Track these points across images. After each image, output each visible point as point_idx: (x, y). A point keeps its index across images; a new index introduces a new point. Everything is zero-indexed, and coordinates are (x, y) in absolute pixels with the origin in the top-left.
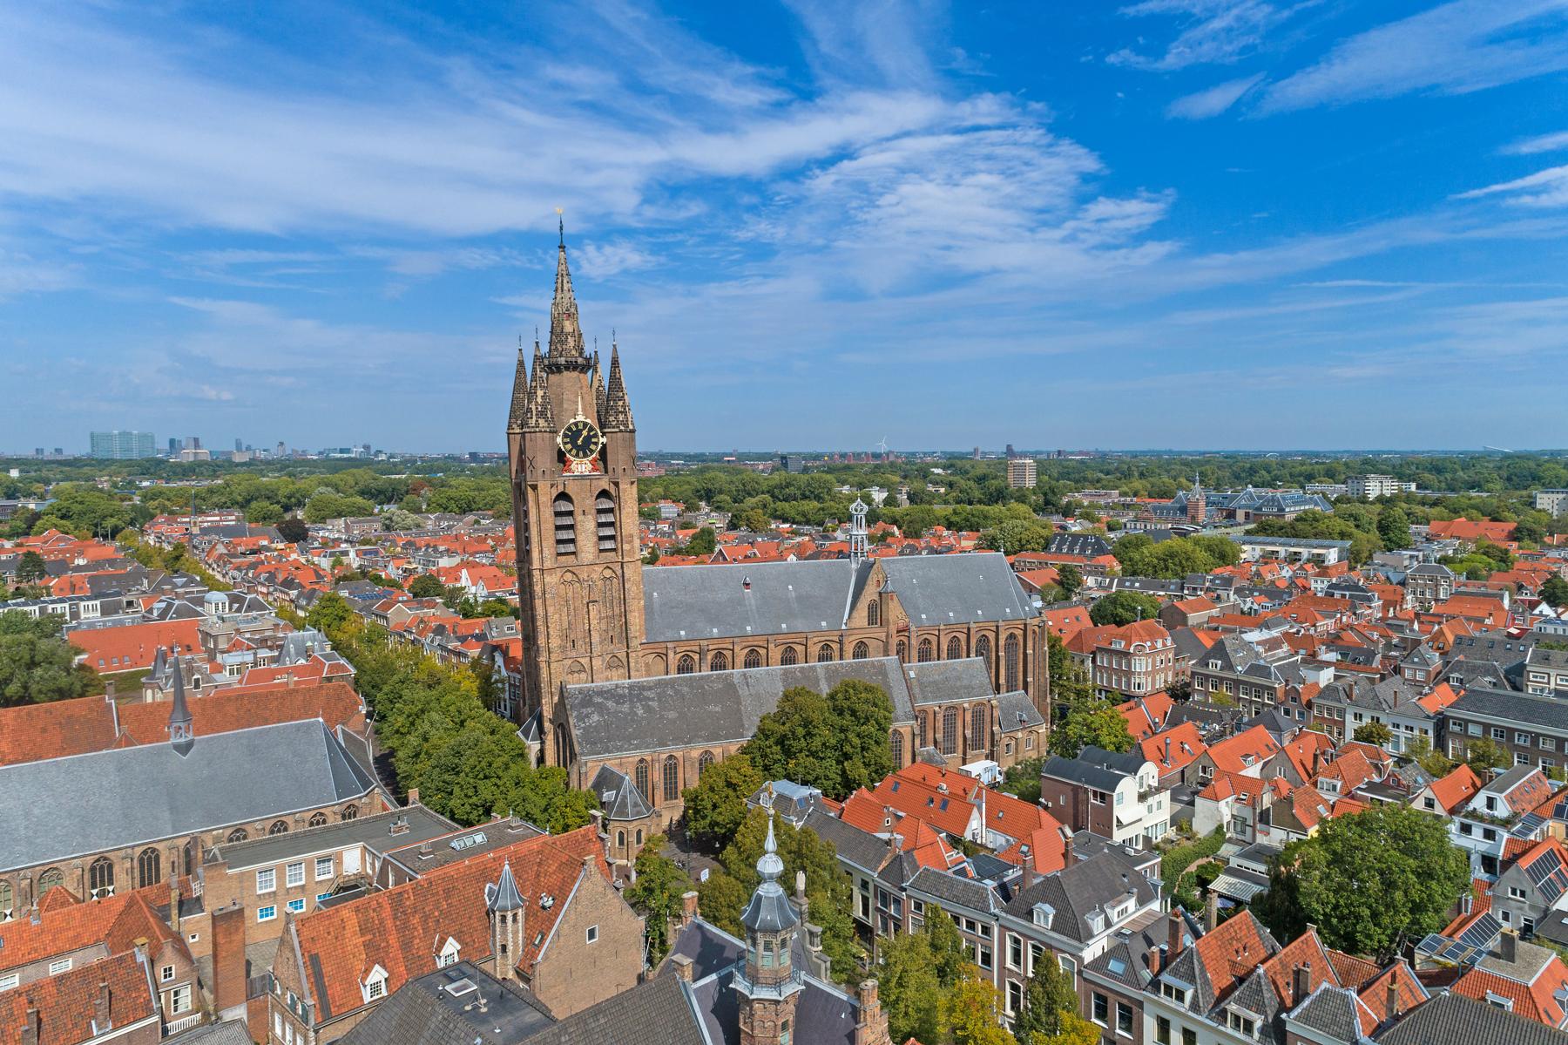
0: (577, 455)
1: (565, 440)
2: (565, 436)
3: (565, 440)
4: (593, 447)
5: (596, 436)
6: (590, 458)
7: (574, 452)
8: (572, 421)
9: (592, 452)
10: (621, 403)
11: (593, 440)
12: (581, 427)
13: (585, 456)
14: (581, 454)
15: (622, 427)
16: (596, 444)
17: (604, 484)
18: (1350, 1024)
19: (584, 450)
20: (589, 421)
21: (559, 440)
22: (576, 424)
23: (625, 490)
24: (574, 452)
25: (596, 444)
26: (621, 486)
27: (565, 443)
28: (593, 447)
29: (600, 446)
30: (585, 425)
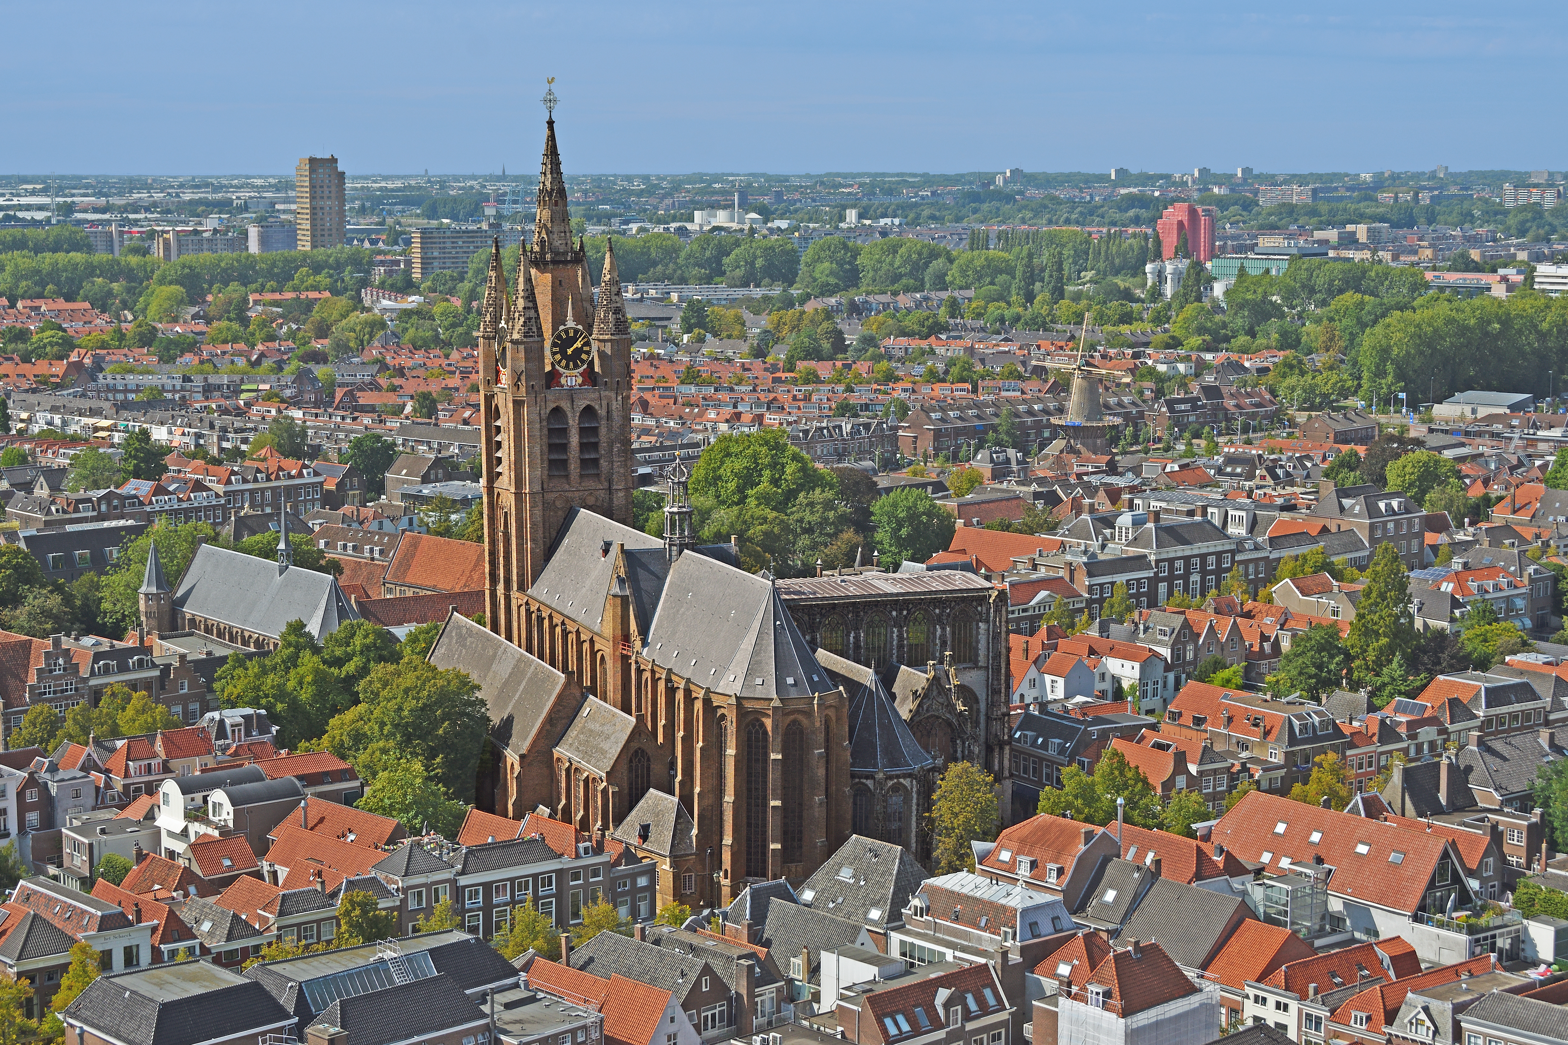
0: (567, 367)
1: (554, 349)
2: (554, 345)
3: (554, 349)
4: (584, 356)
7: (564, 362)
8: (562, 328)
11: (585, 349)
12: (571, 334)
13: (576, 366)
14: (571, 365)
20: (580, 327)
22: (566, 331)
24: (564, 362)
28: (584, 356)
30: (576, 331)
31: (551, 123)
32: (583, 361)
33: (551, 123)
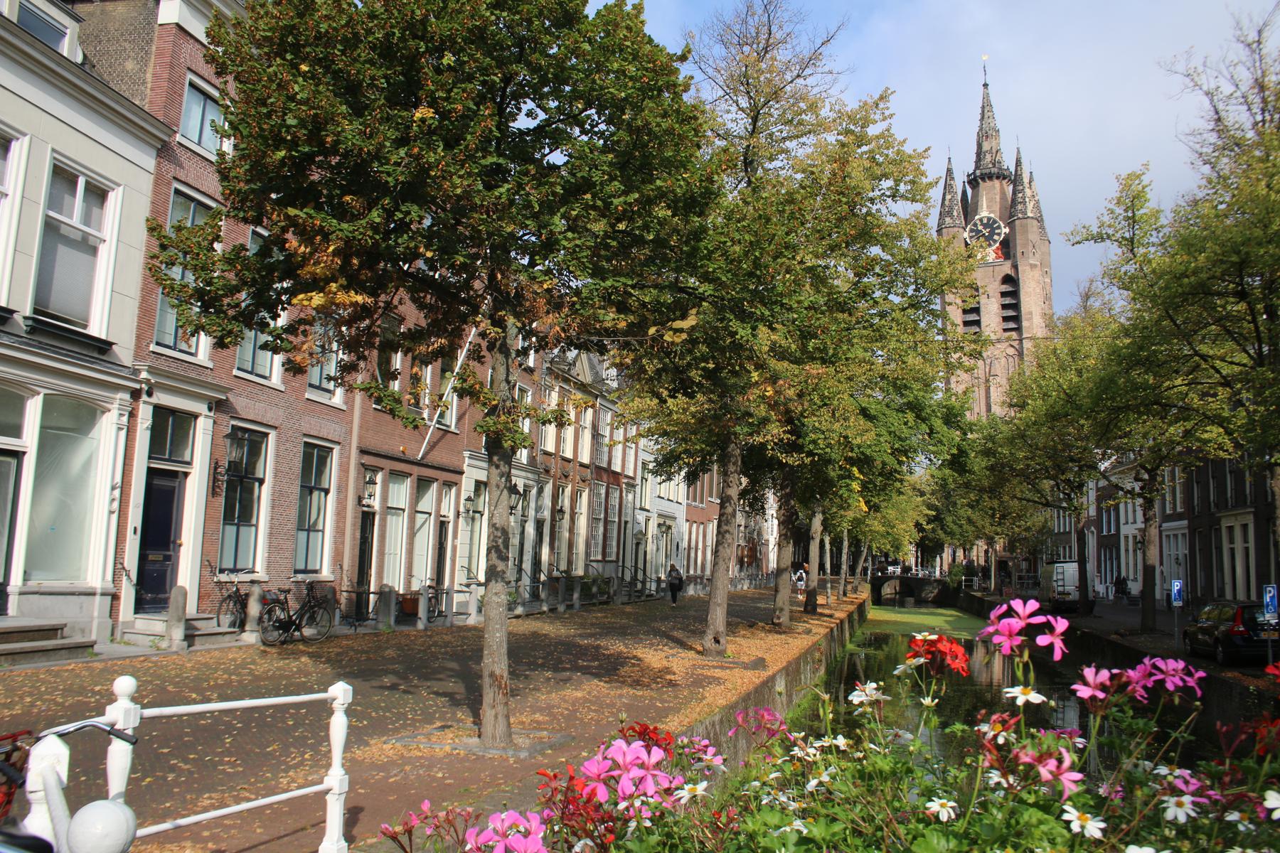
2: (971, 231)
4: (996, 237)
5: (999, 227)
6: (994, 248)
9: (995, 241)
10: (1020, 195)
12: (985, 221)
15: (1020, 215)
16: (999, 234)
17: (1007, 268)
18: (580, 646)
19: (989, 239)
20: (992, 215)
21: (966, 235)
23: (1024, 271)
25: (999, 234)
26: (1020, 268)
27: (971, 237)
29: (1003, 236)
30: (989, 219)
31: (986, 85)
32: (995, 241)
33: (986, 85)
